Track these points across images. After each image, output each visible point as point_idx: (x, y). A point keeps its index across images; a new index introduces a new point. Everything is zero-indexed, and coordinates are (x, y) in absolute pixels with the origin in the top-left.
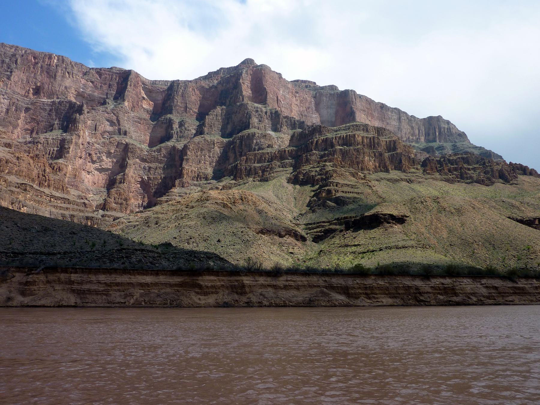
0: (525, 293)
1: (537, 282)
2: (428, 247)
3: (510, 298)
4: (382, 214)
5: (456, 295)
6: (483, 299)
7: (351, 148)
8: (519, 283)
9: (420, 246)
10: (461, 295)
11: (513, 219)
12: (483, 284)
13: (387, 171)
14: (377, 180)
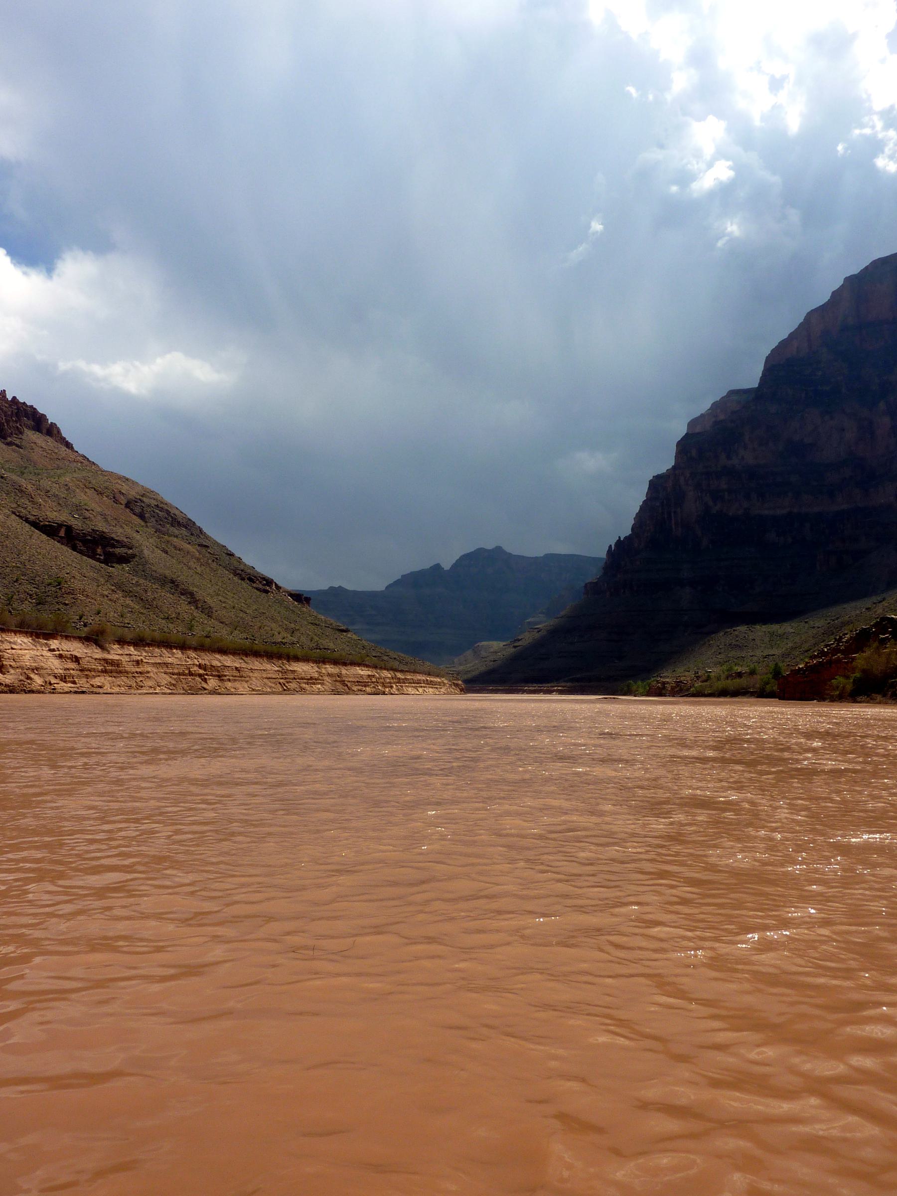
0: (121, 672)
1: (136, 653)
3: (97, 681)
6: (53, 681)
8: (112, 652)
10: (12, 671)
11: (27, 520)
12: (54, 650)
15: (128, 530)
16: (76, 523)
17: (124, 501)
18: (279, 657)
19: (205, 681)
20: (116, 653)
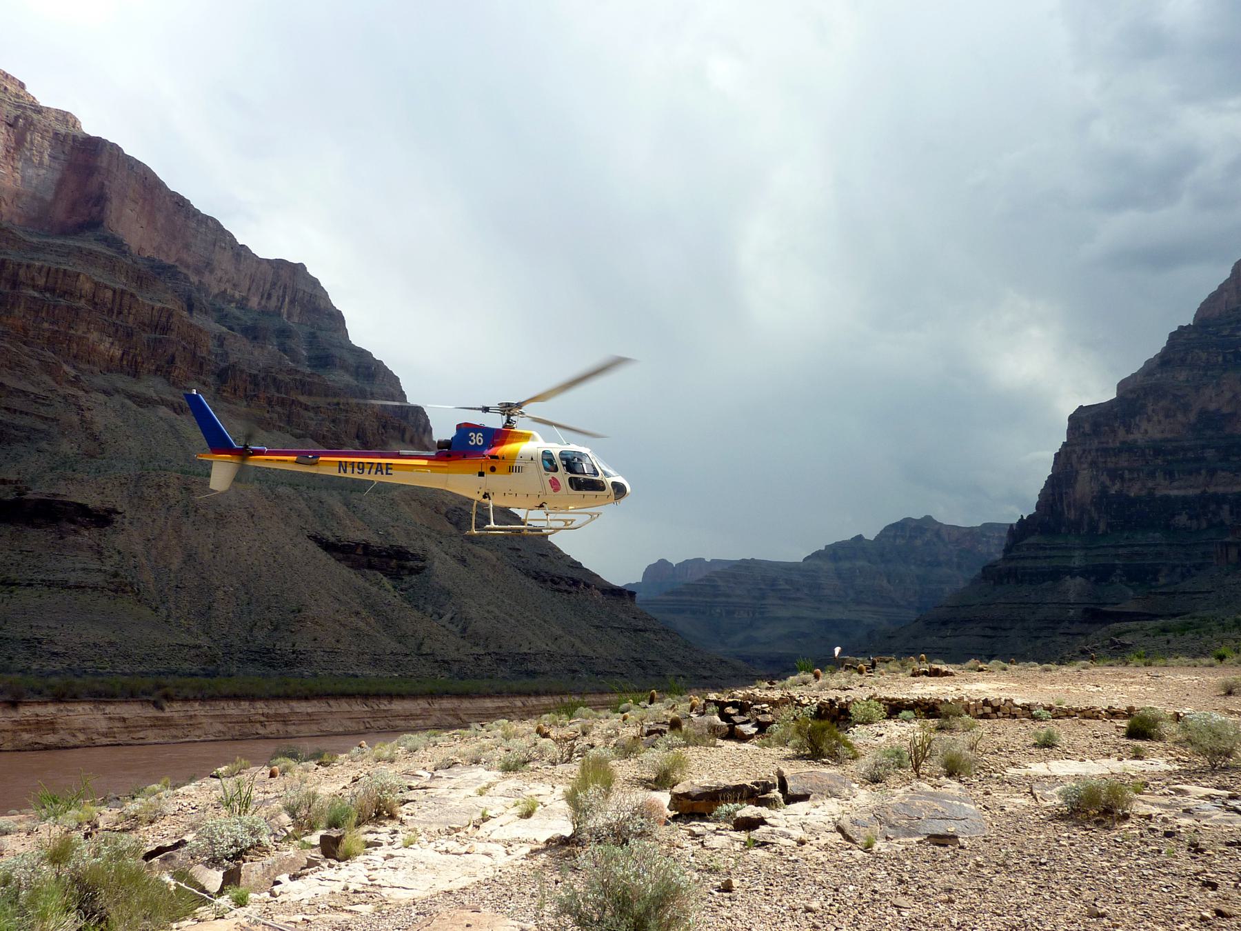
2: (128, 588)
3: (141, 735)
4: (62, 503)
5: (54, 731)
7: (63, 302)
9: (112, 587)
13: (135, 374)
14: (105, 392)
16: (375, 540)
17: (444, 509)
18: (378, 696)
19: (265, 726)
20: (174, 711)
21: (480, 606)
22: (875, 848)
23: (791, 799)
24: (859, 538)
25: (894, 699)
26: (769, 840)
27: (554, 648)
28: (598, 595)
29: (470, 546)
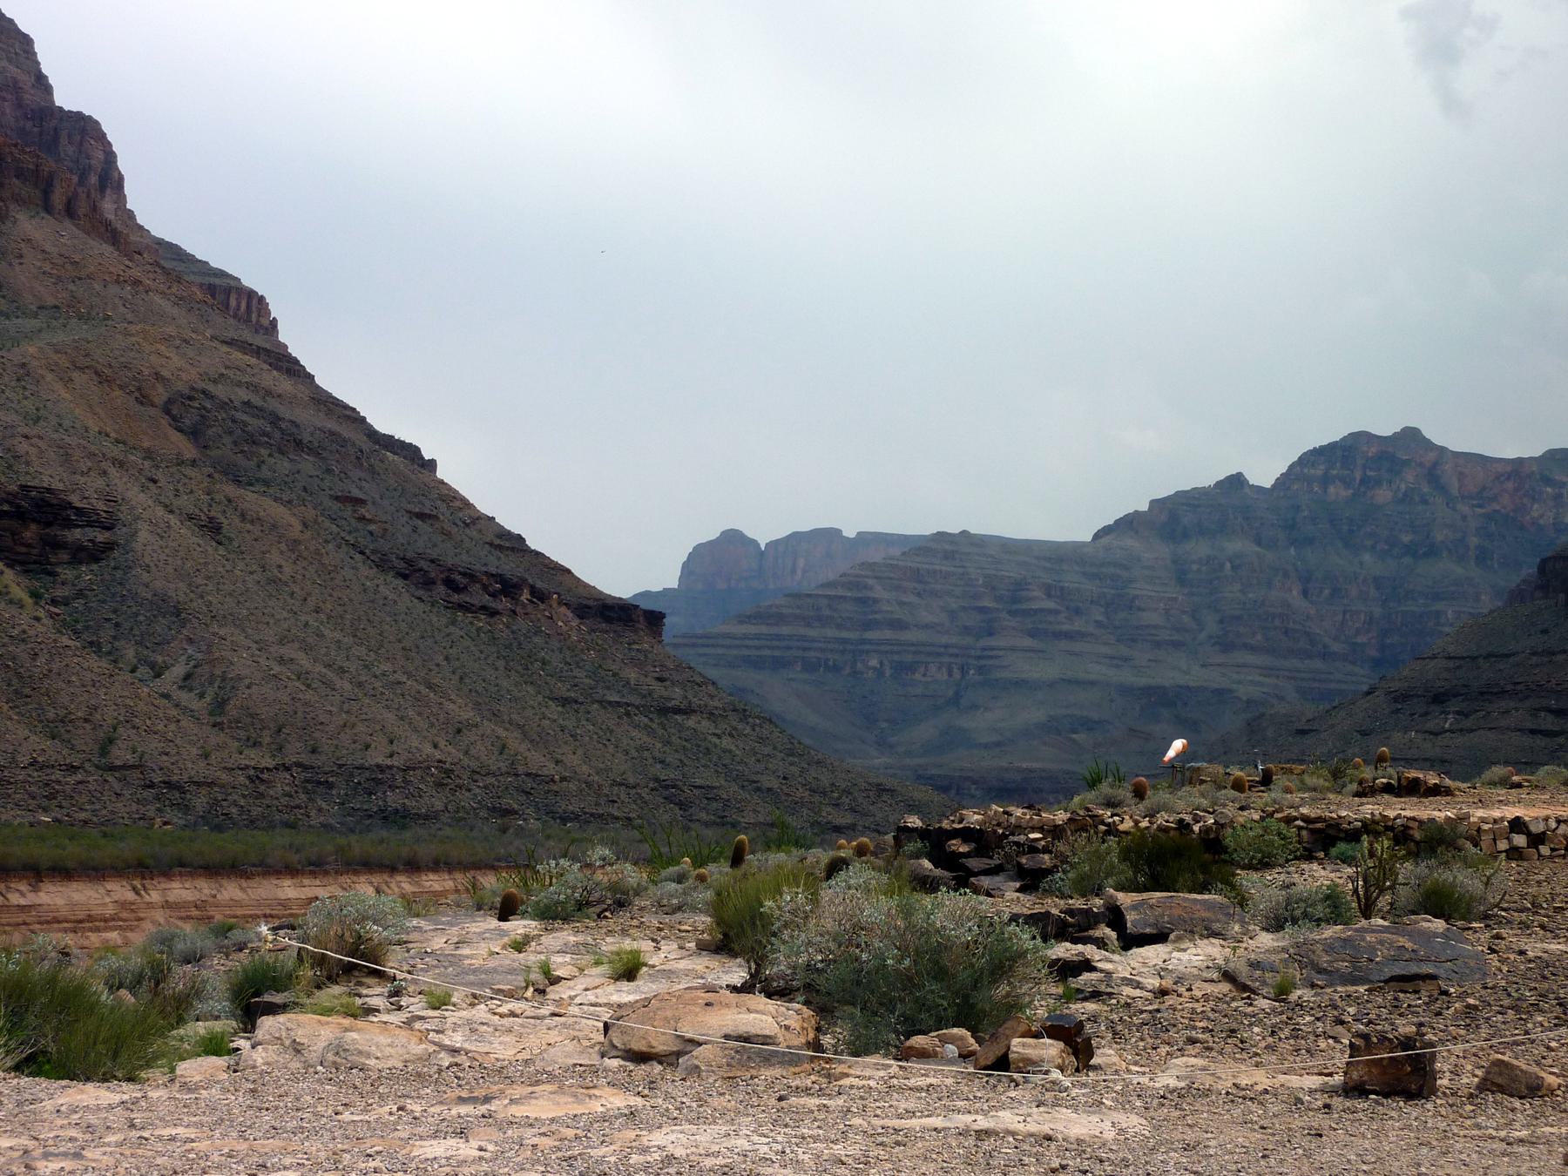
15: (120, 482)
17: (160, 394)
21: (262, 646)
22: (1293, 997)
23: (1130, 941)
24: (1237, 481)
25: (1319, 819)
26: (1103, 988)
27: (451, 753)
28: (565, 619)
29: (231, 490)
